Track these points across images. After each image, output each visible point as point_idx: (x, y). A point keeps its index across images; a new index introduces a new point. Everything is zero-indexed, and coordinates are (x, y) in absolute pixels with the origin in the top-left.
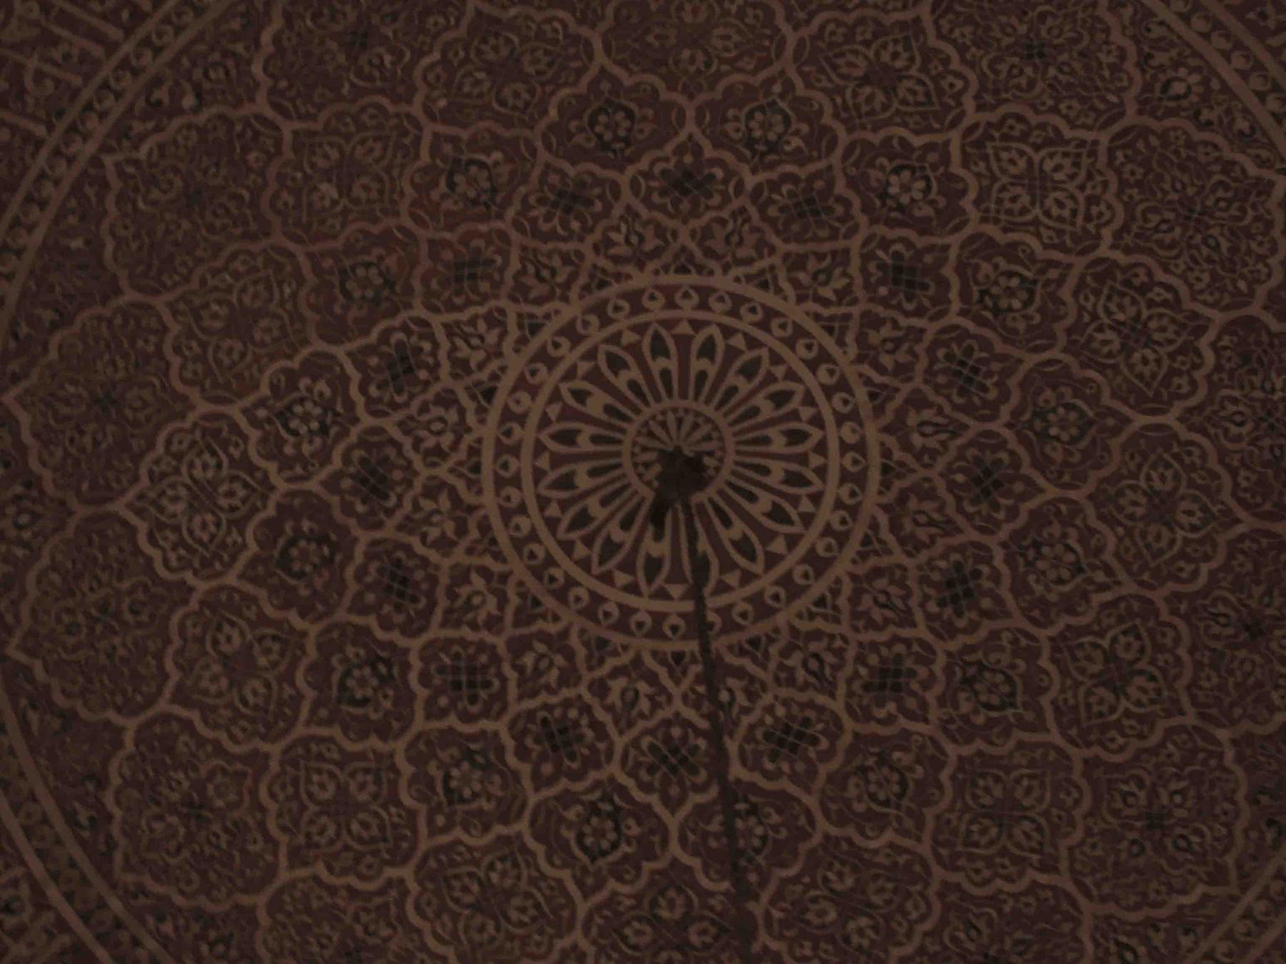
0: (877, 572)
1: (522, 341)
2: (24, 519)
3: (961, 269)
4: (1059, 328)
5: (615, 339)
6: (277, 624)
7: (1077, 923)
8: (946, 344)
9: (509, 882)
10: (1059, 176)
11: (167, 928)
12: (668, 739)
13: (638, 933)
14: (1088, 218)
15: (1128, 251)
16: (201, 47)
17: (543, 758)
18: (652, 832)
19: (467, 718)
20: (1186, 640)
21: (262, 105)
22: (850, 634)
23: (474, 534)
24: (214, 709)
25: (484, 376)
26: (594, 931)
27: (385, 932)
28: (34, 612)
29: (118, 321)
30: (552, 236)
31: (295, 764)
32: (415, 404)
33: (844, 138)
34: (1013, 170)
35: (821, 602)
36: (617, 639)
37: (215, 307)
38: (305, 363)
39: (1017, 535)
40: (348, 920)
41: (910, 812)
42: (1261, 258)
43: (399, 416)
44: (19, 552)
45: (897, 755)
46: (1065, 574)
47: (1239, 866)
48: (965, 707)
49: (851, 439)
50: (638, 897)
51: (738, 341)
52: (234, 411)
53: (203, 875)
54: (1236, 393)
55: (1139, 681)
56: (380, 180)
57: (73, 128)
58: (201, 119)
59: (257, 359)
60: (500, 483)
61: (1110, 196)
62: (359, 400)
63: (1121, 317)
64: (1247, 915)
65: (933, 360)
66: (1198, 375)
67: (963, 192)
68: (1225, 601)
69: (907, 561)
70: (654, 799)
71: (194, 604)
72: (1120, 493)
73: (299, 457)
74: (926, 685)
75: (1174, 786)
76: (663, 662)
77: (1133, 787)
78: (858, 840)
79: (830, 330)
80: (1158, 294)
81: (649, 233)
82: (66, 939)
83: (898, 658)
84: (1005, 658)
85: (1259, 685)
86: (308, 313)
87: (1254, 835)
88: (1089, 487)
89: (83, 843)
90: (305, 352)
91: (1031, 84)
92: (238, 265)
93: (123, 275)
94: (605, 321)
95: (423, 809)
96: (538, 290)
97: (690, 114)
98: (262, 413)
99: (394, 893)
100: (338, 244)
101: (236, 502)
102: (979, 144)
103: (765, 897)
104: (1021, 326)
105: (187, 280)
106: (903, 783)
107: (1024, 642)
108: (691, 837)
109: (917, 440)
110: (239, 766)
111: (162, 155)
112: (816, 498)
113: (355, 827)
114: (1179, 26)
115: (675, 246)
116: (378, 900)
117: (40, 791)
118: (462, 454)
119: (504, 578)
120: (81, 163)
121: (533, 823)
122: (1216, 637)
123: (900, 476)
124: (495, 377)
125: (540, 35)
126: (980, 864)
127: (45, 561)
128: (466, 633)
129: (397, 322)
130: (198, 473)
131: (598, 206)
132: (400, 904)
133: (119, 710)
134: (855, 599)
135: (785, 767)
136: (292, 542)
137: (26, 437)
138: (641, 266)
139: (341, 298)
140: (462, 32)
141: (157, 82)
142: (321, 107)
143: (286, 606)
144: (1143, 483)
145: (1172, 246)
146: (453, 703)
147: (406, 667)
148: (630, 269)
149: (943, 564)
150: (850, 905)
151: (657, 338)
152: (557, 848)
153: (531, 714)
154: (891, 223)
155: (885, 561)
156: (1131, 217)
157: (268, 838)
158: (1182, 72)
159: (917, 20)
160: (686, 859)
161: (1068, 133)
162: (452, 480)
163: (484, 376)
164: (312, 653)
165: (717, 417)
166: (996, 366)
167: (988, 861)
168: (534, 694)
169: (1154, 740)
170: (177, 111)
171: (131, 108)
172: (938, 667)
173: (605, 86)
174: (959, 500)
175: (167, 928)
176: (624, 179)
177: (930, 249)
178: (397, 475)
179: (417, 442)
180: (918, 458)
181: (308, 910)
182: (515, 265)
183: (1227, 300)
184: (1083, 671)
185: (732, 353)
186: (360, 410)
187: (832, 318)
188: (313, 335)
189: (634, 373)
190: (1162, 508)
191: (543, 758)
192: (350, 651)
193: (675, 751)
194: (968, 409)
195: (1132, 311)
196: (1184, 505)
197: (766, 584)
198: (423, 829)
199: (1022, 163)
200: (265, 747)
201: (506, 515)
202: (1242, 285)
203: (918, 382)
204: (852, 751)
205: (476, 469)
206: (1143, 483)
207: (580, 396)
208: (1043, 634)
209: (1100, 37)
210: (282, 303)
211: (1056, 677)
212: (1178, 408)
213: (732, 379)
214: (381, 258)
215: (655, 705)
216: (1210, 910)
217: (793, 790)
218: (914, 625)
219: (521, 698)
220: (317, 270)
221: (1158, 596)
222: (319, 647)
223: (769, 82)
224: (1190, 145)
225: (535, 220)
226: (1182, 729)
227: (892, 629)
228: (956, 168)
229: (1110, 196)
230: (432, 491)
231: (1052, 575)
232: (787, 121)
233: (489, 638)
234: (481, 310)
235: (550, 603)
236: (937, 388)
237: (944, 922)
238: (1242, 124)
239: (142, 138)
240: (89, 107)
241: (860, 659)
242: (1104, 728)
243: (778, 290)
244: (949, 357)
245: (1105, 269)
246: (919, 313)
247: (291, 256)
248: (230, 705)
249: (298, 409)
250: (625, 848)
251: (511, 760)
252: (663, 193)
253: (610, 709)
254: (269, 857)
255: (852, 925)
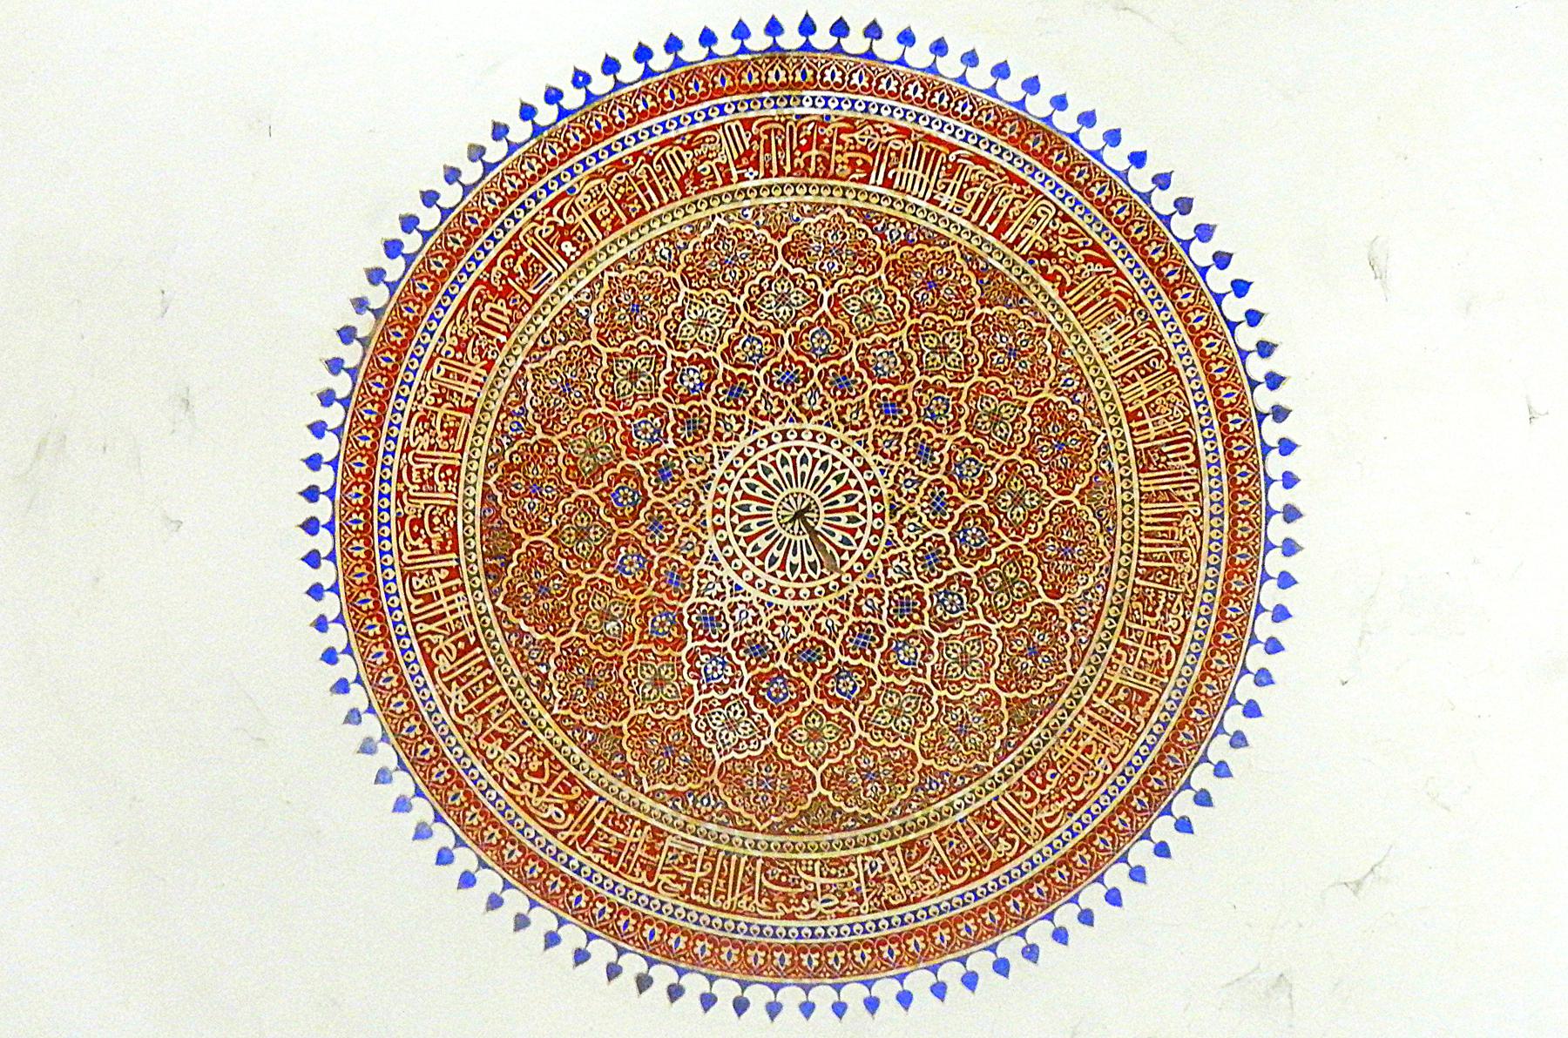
0: (875, 443)
1: (718, 566)
2: (705, 801)
3: (736, 366)
4: (774, 331)
5: (734, 526)
6: (803, 712)
7: (1051, 401)
8: (772, 382)
9: (959, 650)
10: (700, 313)
11: (914, 805)
12: (921, 559)
13: (1001, 600)
14: (723, 306)
15: (742, 292)
16: (519, 657)
17: (910, 617)
18: (960, 579)
19: (879, 645)
20: (933, 315)
21: (558, 641)
22: (899, 463)
23: (800, 615)
24: (829, 752)
25: (728, 588)
26: (994, 619)
27: (959, 711)
28: (749, 812)
29: (634, 732)
30: (671, 539)
31: (868, 726)
32: (729, 620)
33: (661, 400)
34: (693, 331)
35: (882, 471)
36: (871, 567)
37: (646, 691)
38: (689, 661)
39: (870, 376)
40: (946, 726)
41: (985, 461)
42: (754, 237)
43: (731, 628)
44: (719, 808)
45: (958, 459)
46: (892, 360)
47: (1037, 321)
48: (944, 421)
49: (810, 436)
50: (986, 594)
51: (752, 472)
52: (698, 698)
53: (899, 781)
54: (818, 263)
55: (947, 341)
56: (614, 603)
57: (534, 721)
58: (553, 667)
59: (677, 681)
60: (782, 596)
61: (714, 294)
62: (717, 644)
63: (773, 303)
64: (1060, 323)
65: (779, 390)
66: (807, 277)
67: (699, 355)
68: (917, 292)
69: (873, 427)
70: (946, 573)
71: (779, 745)
72: (858, 325)
73: (731, 678)
74: (930, 436)
75: (998, 340)
76: (888, 550)
77: (996, 358)
78: (991, 488)
79: (755, 431)
80: (765, 285)
81: (685, 496)
82: (899, 849)
83: (915, 445)
84: (926, 397)
85: (957, 289)
86: (666, 652)
87: (1025, 310)
88: (853, 338)
89: (861, 827)
90: (684, 660)
91: (650, 313)
92: (630, 676)
93: (613, 723)
94: (724, 527)
95: (912, 677)
96: (697, 551)
97: (630, 462)
98: (704, 687)
99: (944, 703)
100: (639, 630)
101: (740, 711)
102: (676, 343)
103: (1003, 537)
104: (769, 347)
105: (628, 698)
106: (971, 460)
107: (920, 387)
108: (968, 562)
109: (817, 407)
110: (859, 750)
111: (564, 688)
112: (835, 459)
113: (907, 709)
114: (633, 246)
115: (697, 488)
116: (943, 711)
117: (829, 837)
118: (761, 608)
119: (825, 607)
120: (552, 723)
121: (937, 631)
122: (933, 302)
123: (832, 419)
124: (731, 583)
125: (570, 515)
126: (1015, 436)
127: (729, 801)
128: (841, 633)
129: (687, 617)
130: (719, 723)
131: (664, 514)
132: (948, 701)
133: (810, 792)
134: (885, 456)
135: (950, 510)
136: (769, 694)
137: (669, 788)
138: (701, 504)
139: (666, 636)
140: (556, 547)
141: (528, 680)
142: (569, 616)
143: (797, 707)
144: (855, 314)
145: (742, 272)
146: (870, 647)
147: (847, 664)
148: (700, 509)
149: (877, 413)
150: (1018, 500)
151: (739, 507)
152: (952, 623)
153: (890, 616)
154: (708, 389)
155: (871, 438)
156: (726, 287)
157: (896, 749)
158: (657, 249)
159: (608, 354)
160: (977, 568)
161: (679, 304)
162: (771, 616)
163: (728, 588)
164: (824, 702)
165: (786, 492)
166: (787, 363)
167: (1015, 432)
168: (881, 611)
169: (976, 342)
170: (546, 677)
171: (535, 694)
172: (923, 428)
173: (604, 494)
174: (849, 396)
175: (914, 805)
176: (654, 499)
177: (724, 377)
178: (759, 639)
179: (747, 625)
180: (825, 409)
181: (935, 742)
182: (681, 558)
183: (773, 256)
184: (938, 365)
185: (757, 476)
186: (722, 645)
187: (750, 428)
188: (678, 654)
189: (754, 522)
190: (868, 309)
191: (910, 617)
192: (829, 685)
193: (928, 558)
194: (806, 381)
195: (771, 298)
196: (868, 299)
197: (868, 493)
198: (921, 680)
199: (689, 327)
200: (856, 736)
201: (797, 597)
202: (767, 248)
203: (789, 400)
204: (952, 479)
205: (770, 604)
206: (855, 314)
207: (755, 548)
208: (918, 378)
209: (633, 279)
210: (657, 662)
211: (939, 377)
212: (821, 289)
213: (770, 480)
214: (653, 614)
215: (906, 559)
216: (1056, 340)
217: (961, 510)
218: (901, 434)
219: (880, 618)
220: (648, 642)
221: (910, 322)
222: (822, 697)
223: (624, 424)
224: (694, 254)
225: (661, 543)
226: (972, 328)
227: (902, 444)
228: (687, 356)
229: (714, 294)
230: (773, 627)
231: (892, 366)
232: (646, 422)
233: (849, 623)
234: (696, 578)
235: (844, 591)
236: (793, 391)
237: (1037, 460)
238: (688, 230)
239: (551, 693)
240: (527, 711)
241: (912, 462)
242: (966, 363)
243: (730, 448)
244: (779, 382)
245: (749, 304)
246: (754, 389)
247: (635, 652)
248: (830, 745)
249: (709, 671)
250: (963, 594)
251: (904, 631)
252: (667, 484)
253: (900, 580)
254: (905, 751)
255: (1027, 502)
